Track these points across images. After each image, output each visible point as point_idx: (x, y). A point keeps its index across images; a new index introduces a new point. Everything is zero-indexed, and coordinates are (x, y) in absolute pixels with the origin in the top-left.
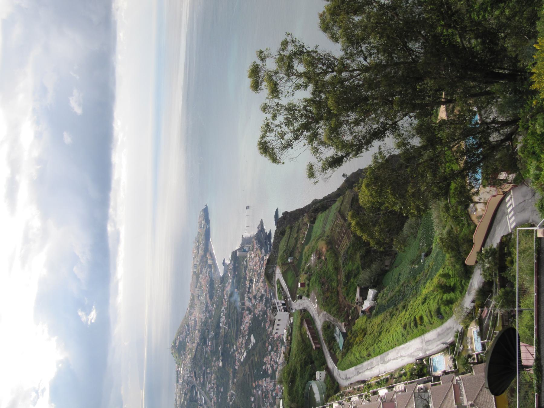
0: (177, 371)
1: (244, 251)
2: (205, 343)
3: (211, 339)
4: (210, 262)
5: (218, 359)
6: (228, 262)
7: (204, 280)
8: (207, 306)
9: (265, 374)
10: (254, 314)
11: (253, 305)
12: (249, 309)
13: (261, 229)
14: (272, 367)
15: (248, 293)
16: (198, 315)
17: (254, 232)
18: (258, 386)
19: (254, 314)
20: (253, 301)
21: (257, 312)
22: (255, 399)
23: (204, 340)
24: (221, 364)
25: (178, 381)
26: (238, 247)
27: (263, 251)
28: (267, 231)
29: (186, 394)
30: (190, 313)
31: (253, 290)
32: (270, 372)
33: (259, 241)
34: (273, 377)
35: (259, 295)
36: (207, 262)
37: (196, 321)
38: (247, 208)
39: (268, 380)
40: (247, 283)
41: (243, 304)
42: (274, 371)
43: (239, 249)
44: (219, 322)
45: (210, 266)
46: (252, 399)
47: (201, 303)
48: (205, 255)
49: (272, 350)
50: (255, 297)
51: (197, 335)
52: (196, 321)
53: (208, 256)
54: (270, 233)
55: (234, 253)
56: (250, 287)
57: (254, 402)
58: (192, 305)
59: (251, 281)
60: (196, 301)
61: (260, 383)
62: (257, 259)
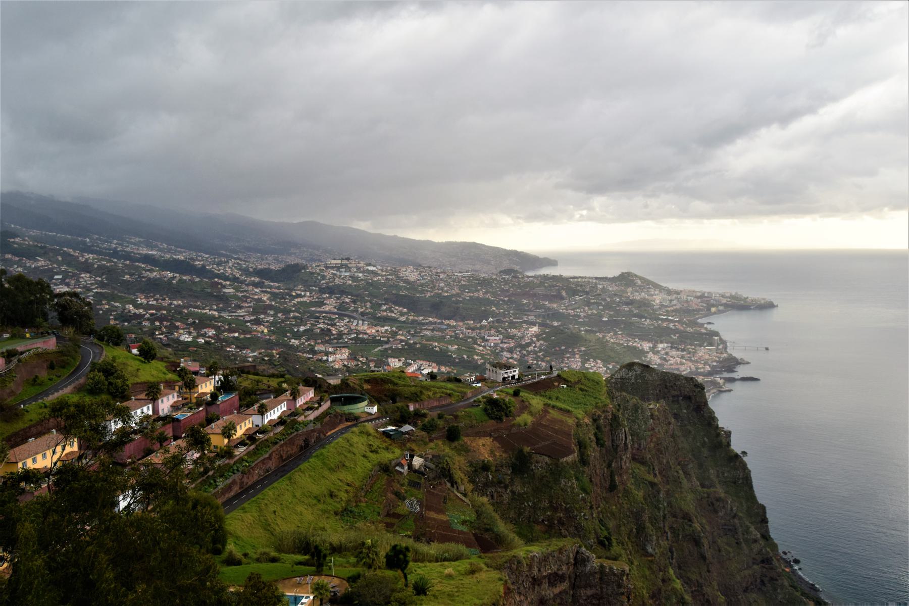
0: (606, 278)
1: (718, 345)
2: (627, 304)
3: (630, 311)
4: (713, 309)
5: (610, 316)
6: (709, 327)
7: (695, 304)
8: (667, 306)
9: (585, 361)
10: (648, 352)
11: (658, 352)
12: (655, 346)
15: (672, 347)
16: (658, 299)
17: (738, 355)
18: (574, 354)
20: (663, 352)
21: (650, 355)
23: (631, 303)
24: (605, 319)
25: (596, 278)
26: (724, 338)
27: (715, 364)
29: (581, 286)
30: (661, 289)
31: (674, 352)
33: (725, 360)
36: (713, 306)
37: (652, 295)
38: (767, 349)
39: (579, 363)
41: (662, 342)
43: (721, 339)
44: (646, 318)
45: (709, 310)
47: (671, 301)
48: (722, 305)
49: (608, 368)
51: (637, 297)
52: (652, 295)
53: (721, 308)
54: (734, 372)
55: (717, 334)
56: (678, 349)
58: (669, 292)
59: (683, 350)
60: (675, 295)
61: (577, 356)
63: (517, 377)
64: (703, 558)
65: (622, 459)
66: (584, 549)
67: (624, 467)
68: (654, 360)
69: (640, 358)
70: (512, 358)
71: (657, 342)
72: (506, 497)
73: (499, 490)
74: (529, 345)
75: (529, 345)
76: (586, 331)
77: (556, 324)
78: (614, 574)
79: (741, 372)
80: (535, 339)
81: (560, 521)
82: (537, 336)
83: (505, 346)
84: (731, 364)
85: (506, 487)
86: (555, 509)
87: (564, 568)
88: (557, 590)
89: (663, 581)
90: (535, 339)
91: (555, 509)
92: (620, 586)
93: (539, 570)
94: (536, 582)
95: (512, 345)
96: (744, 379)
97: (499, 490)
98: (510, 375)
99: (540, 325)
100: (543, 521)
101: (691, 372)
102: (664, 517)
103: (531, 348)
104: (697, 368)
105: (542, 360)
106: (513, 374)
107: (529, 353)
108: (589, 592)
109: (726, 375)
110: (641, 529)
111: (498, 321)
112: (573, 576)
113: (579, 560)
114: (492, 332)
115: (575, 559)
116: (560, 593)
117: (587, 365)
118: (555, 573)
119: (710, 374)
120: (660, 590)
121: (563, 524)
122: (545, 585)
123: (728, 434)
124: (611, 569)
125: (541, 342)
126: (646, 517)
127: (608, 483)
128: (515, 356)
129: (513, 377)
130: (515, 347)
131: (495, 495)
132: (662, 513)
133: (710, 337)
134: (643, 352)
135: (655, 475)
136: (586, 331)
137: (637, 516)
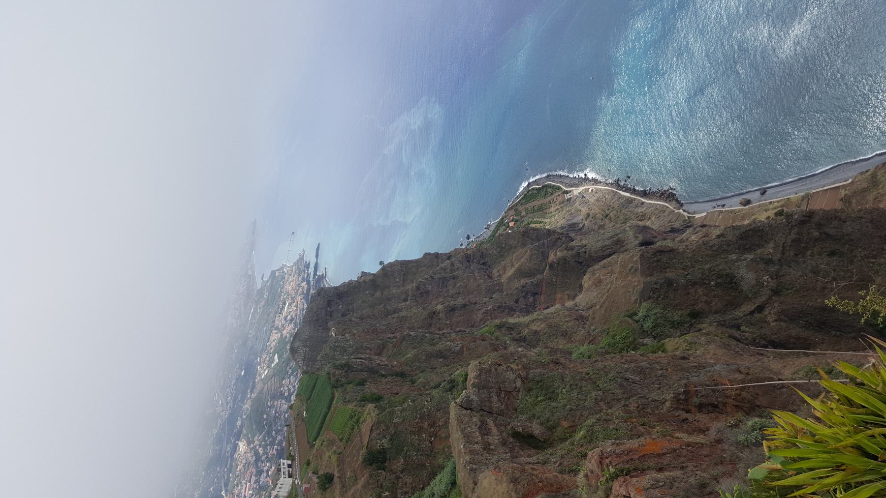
10: (282, 335)
11: (283, 326)
12: (277, 329)
13: (302, 258)
14: (289, 390)
19: (282, 335)
21: (285, 332)
22: (267, 417)
28: (307, 259)
32: (286, 394)
34: (288, 399)
35: (289, 317)
38: (293, 233)
39: (283, 401)
40: (281, 303)
41: (274, 322)
42: (290, 395)
46: (265, 416)
49: (292, 374)
50: (285, 318)
55: (273, 273)
56: (283, 308)
57: (266, 420)
59: (284, 304)
62: (293, 283)
63: (290, 462)
64: (464, 306)
65: (379, 364)
66: (458, 400)
67: (386, 363)
68: (289, 330)
69: (287, 343)
70: (268, 471)
71: (273, 326)
72: (409, 479)
73: (400, 485)
74: (256, 453)
75: (256, 453)
76: (252, 392)
77: (239, 423)
78: (480, 375)
79: (311, 258)
80: (252, 446)
81: (432, 425)
82: (249, 443)
83: (253, 477)
84: (302, 265)
85: (398, 478)
86: (421, 429)
87: (475, 419)
88: (494, 430)
89: (483, 340)
90: (252, 446)
91: (421, 429)
92: (490, 371)
93: (477, 443)
94: (487, 447)
95: (254, 470)
96: (317, 256)
97: (400, 485)
98: (287, 469)
99: (238, 439)
100: (431, 442)
101: (307, 300)
102: (430, 333)
103: (261, 451)
104: (303, 293)
105: (274, 439)
106: (286, 466)
107: (265, 453)
108: (495, 399)
109: (311, 270)
110: (441, 355)
111: (226, 485)
112: (481, 413)
113: (467, 406)
114: (236, 492)
115: (466, 409)
116: (496, 425)
117: (286, 394)
118: (479, 428)
119: (308, 283)
120: (491, 345)
121: (434, 423)
122: (490, 439)
123: (364, 274)
124: (476, 377)
125: (256, 438)
126: (429, 348)
127: (399, 379)
128: (266, 469)
129: (289, 466)
130: (257, 467)
131: (405, 490)
132: (428, 335)
133: (277, 279)
134: (282, 340)
135: (395, 337)
136: (252, 392)
137: (430, 356)
